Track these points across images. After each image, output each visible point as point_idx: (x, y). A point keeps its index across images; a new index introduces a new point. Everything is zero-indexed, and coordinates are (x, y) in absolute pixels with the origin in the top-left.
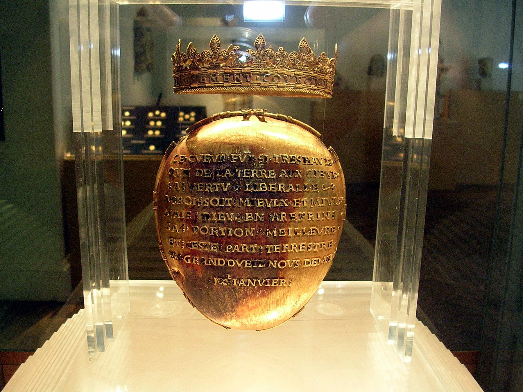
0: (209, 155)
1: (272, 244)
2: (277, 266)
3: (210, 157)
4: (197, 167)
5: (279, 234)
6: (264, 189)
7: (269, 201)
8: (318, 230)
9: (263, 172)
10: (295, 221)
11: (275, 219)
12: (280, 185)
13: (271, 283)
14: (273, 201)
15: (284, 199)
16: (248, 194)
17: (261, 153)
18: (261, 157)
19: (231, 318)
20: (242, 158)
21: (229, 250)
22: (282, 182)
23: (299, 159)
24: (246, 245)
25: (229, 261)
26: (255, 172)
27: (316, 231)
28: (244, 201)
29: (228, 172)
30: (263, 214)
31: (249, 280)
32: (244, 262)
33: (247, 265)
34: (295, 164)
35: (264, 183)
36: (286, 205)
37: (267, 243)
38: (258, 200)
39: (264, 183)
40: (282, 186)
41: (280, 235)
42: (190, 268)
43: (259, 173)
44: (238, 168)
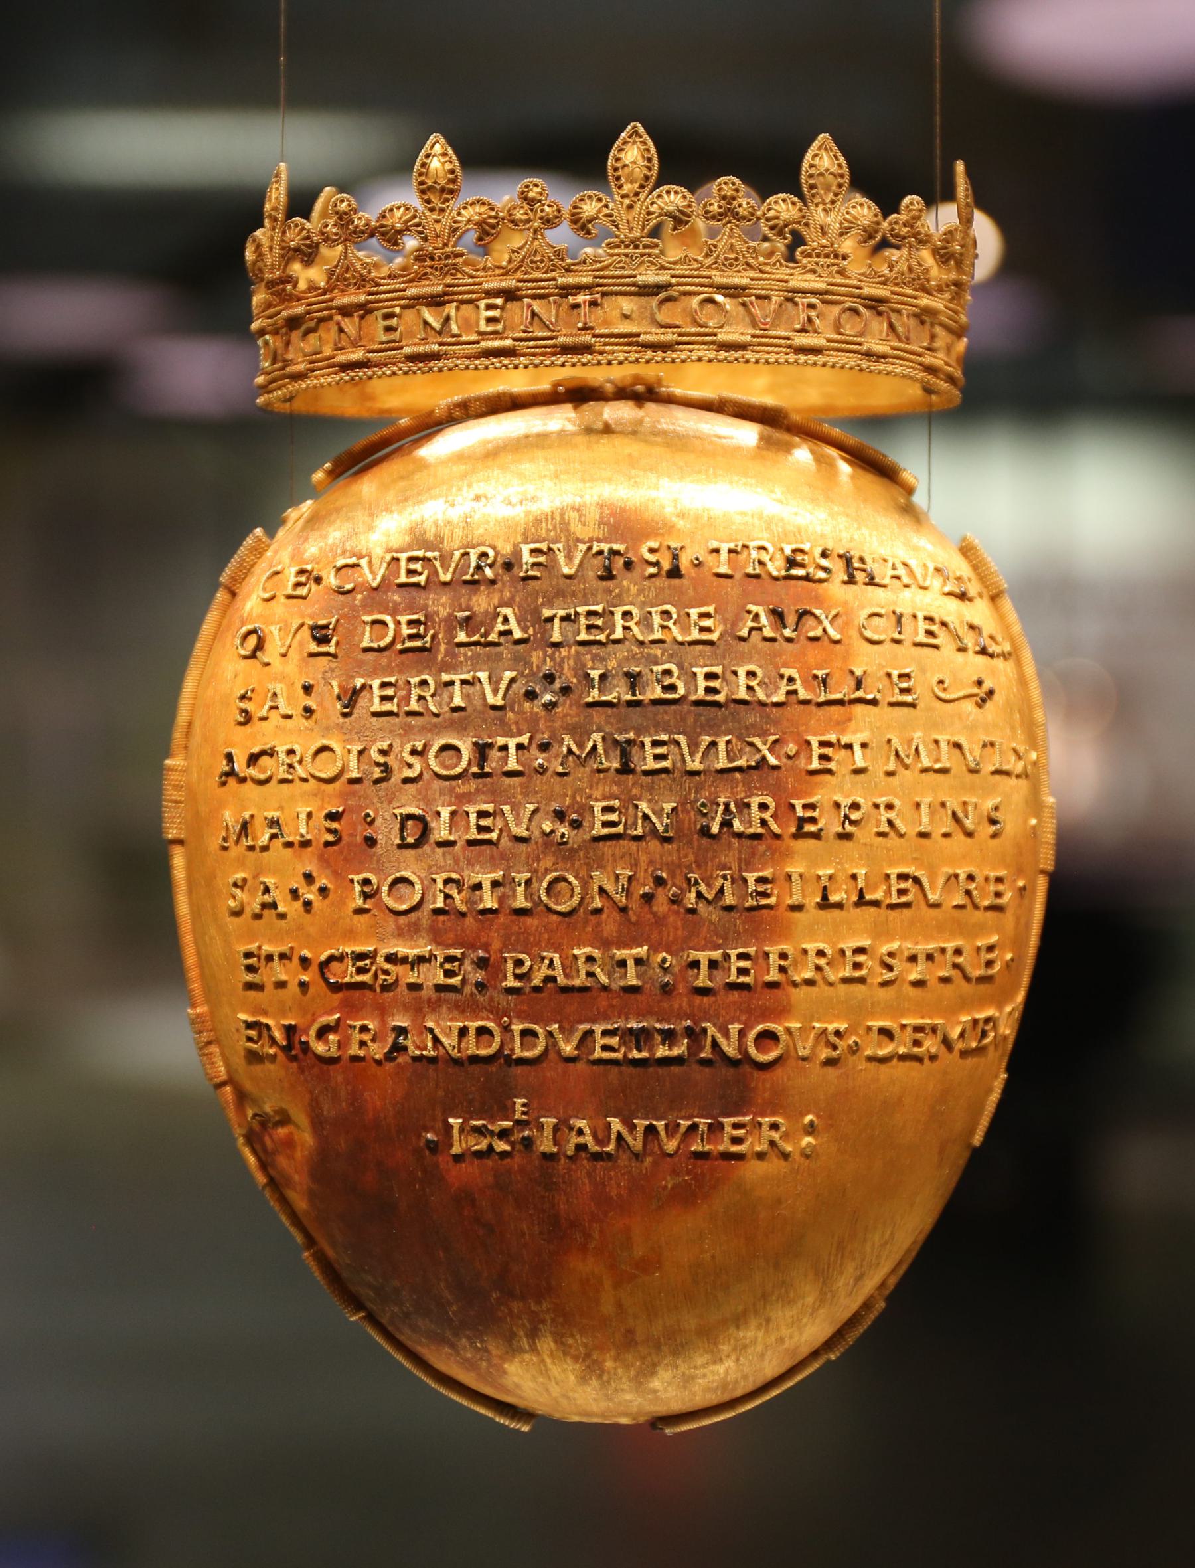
0: (420, 553)
1: (716, 947)
2: (742, 1047)
3: (424, 559)
4: (367, 607)
5: (744, 896)
6: (672, 688)
7: (694, 745)
8: (925, 881)
9: (666, 614)
10: (816, 836)
11: (726, 824)
12: (742, 672)
13: (716, 1128)
14: (713, 744)
15: (763, 734)
16: (597, 715)
17: (648, 537)
18: (652, 550)
19: (533, 1334)
20: (569, 557)
21: (517, 977)
22: (750, 662)
23: (824, 562)
24: (596, 953)
25: (517, 1027)
26: (627, 615)
27: (917, 880)
28: (581, 746)
29: (506, 620)
30: (668, 807)
31: (616, 1124)
32: (590, 1032)
33: (605, 1048)
34: (807, 578)
35: (673, 667)
36: (773, 761)
37: (691, 939)
38: (647, 741)
39: (673, 667)
40: (751, 674)
41: (750, 902)
42: (337, 1075)
43: (646, 622)
44: (550, 604)
